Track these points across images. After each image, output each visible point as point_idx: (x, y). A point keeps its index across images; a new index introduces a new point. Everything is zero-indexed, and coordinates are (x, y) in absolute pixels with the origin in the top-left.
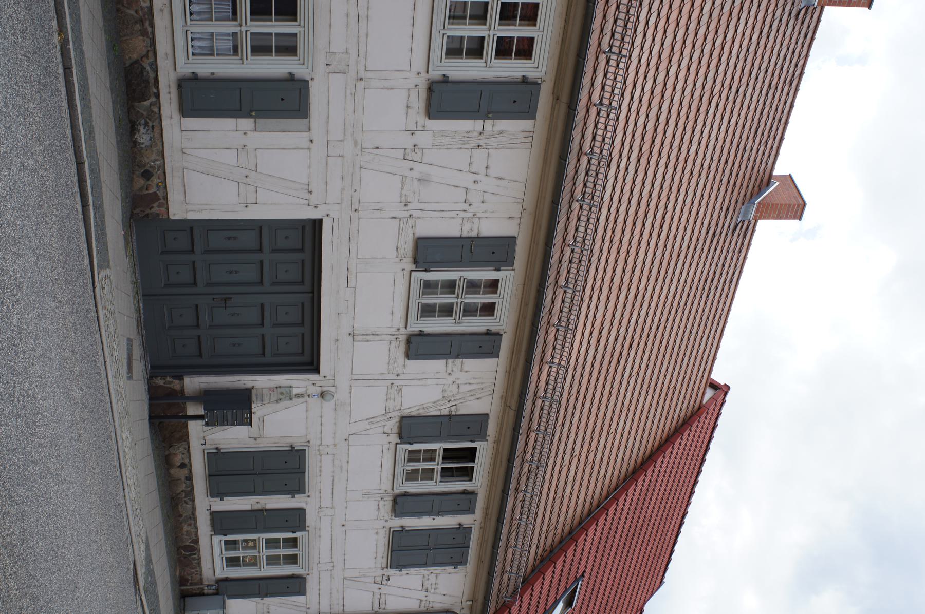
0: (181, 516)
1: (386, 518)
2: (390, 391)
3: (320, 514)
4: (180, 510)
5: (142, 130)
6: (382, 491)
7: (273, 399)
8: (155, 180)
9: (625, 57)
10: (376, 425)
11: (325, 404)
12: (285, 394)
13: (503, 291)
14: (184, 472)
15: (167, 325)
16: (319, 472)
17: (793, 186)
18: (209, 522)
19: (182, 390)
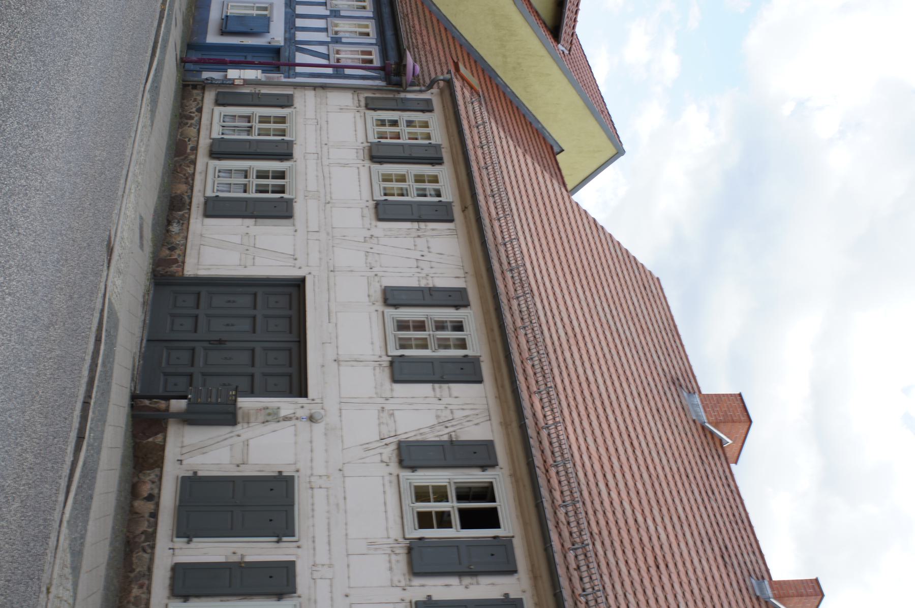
0: (132, 571)
1: (403, 584)
2: (381, 414)
3: (316, 575)
4: (135, 560)
5: (175, 225)
6: (391, 541)
7: (261, 418)
8: (178, 252)
9: (599, 591)
10: (372, 452)
11: (316, 426)
12: (272, 416)
13: (471, 330)
14: (150, 506)
15: (163, 365)
16: (311, 508)
17: (742, 438)
18: (167, 582)
19: (167, 409)
